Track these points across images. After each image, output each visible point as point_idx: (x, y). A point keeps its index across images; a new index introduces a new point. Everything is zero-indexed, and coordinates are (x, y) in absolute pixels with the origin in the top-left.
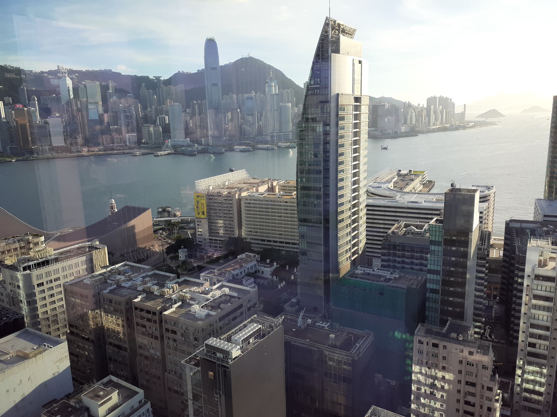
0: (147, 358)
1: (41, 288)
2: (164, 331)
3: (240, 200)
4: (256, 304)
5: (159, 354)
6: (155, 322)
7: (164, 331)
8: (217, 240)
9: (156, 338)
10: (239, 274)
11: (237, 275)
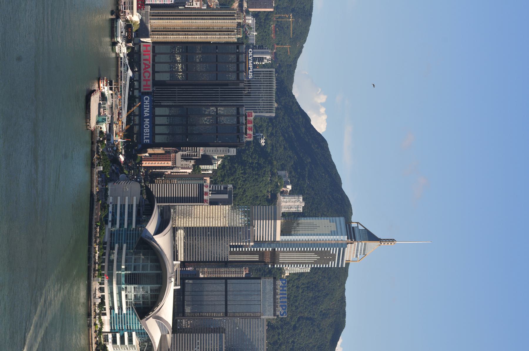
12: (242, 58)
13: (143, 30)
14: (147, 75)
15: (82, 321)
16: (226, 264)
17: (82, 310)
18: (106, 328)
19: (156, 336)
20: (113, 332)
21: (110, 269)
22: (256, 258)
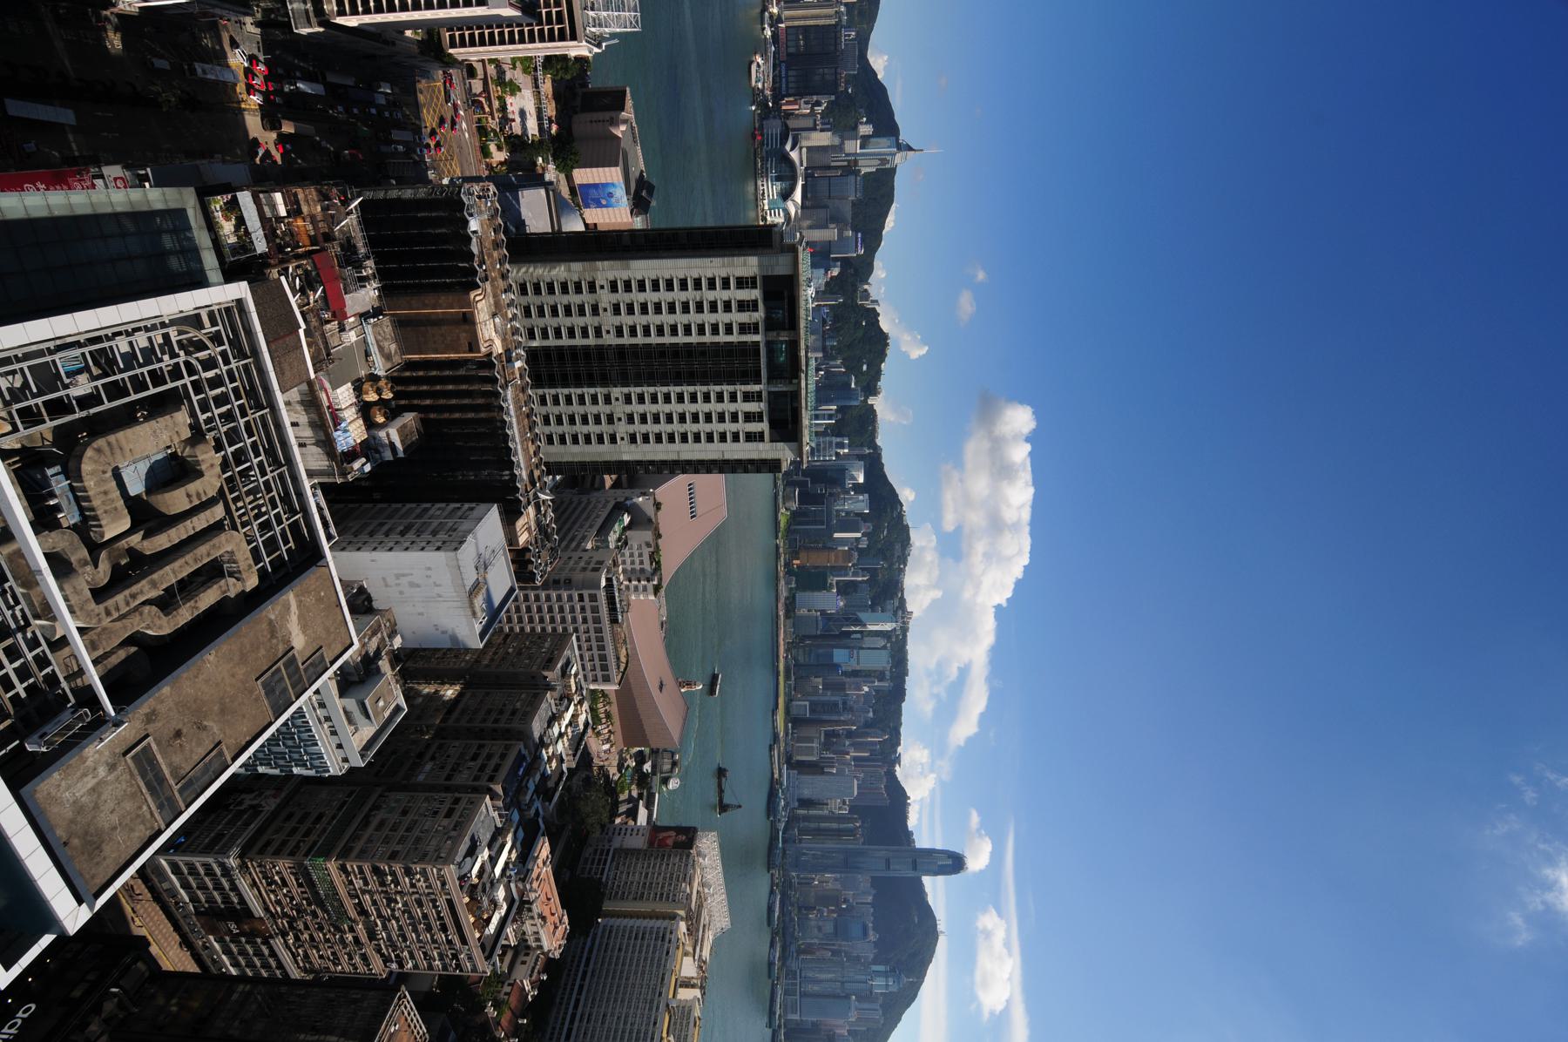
0: (421, 756)
1: (576, 598)
2: (457, 795)
3: (673, 917)
4: (461, 970)
5: (421, 778)
6: (476, 778)
7: (457, 795)
8: (605, 864)
9: (449, 778)
10: (530, 914)
11: (530, 910)
12: (838, 34)
13: (779, 20)
14: (783, 49)
15: (752, 205)
16: (829, 168)
17: (752, 197)
18: (766, 207)
19: (792, 211)
20: (770, 209)
21: (767, 173)
22: (846, 163)
